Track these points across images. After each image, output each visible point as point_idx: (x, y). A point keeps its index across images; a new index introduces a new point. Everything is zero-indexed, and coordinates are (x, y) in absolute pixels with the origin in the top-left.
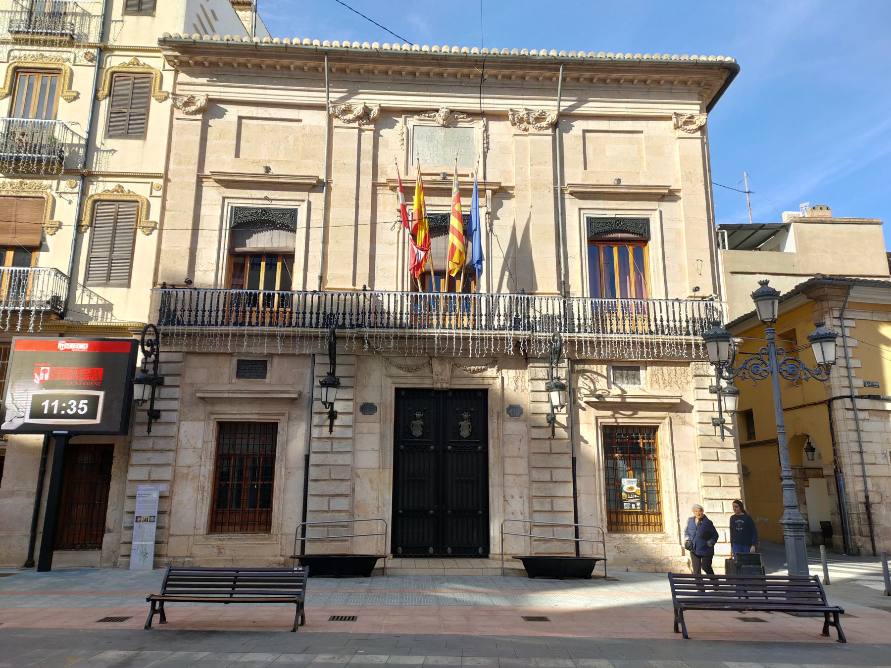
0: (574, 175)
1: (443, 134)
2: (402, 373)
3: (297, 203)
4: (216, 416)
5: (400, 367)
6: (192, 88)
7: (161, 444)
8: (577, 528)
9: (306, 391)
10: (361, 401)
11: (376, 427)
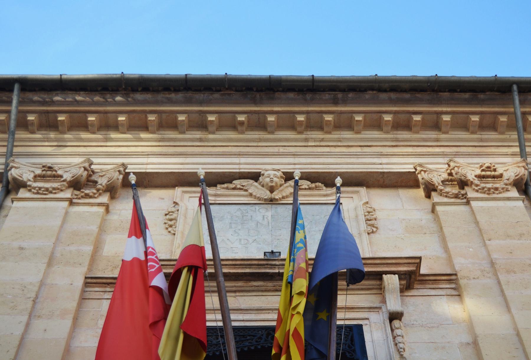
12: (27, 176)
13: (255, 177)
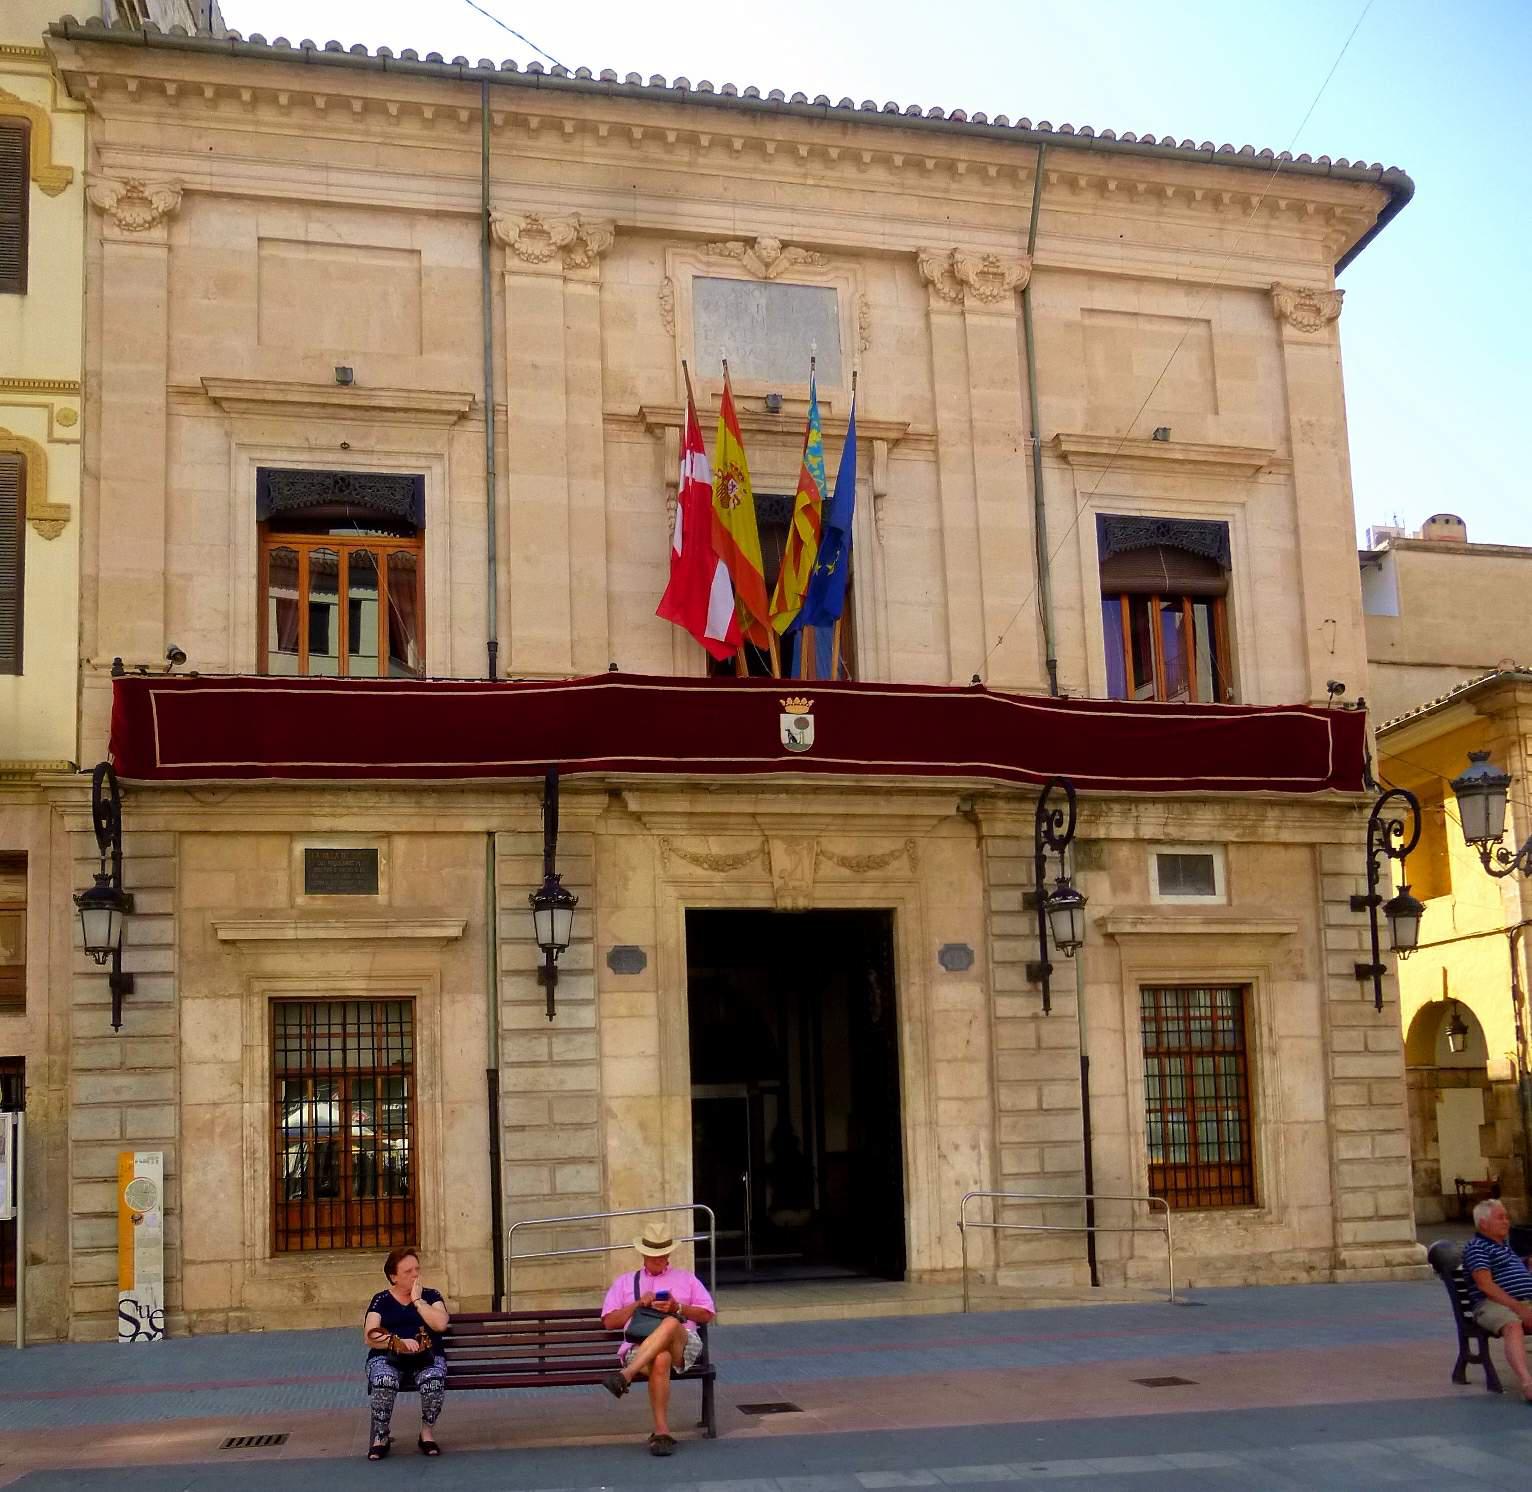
0: (1062, 415)
1: (763, 302)
2: (700, 872)
3: (423, 462)
4: (265, 985)
5: (696, 860)
6: (137, 160)
7: (144, 1054)
8: (1090, 1204)
9: (478, 919)
10: (609, 944)
11: (648, 1002)
12: (513, 236)
13: (750, 242)
